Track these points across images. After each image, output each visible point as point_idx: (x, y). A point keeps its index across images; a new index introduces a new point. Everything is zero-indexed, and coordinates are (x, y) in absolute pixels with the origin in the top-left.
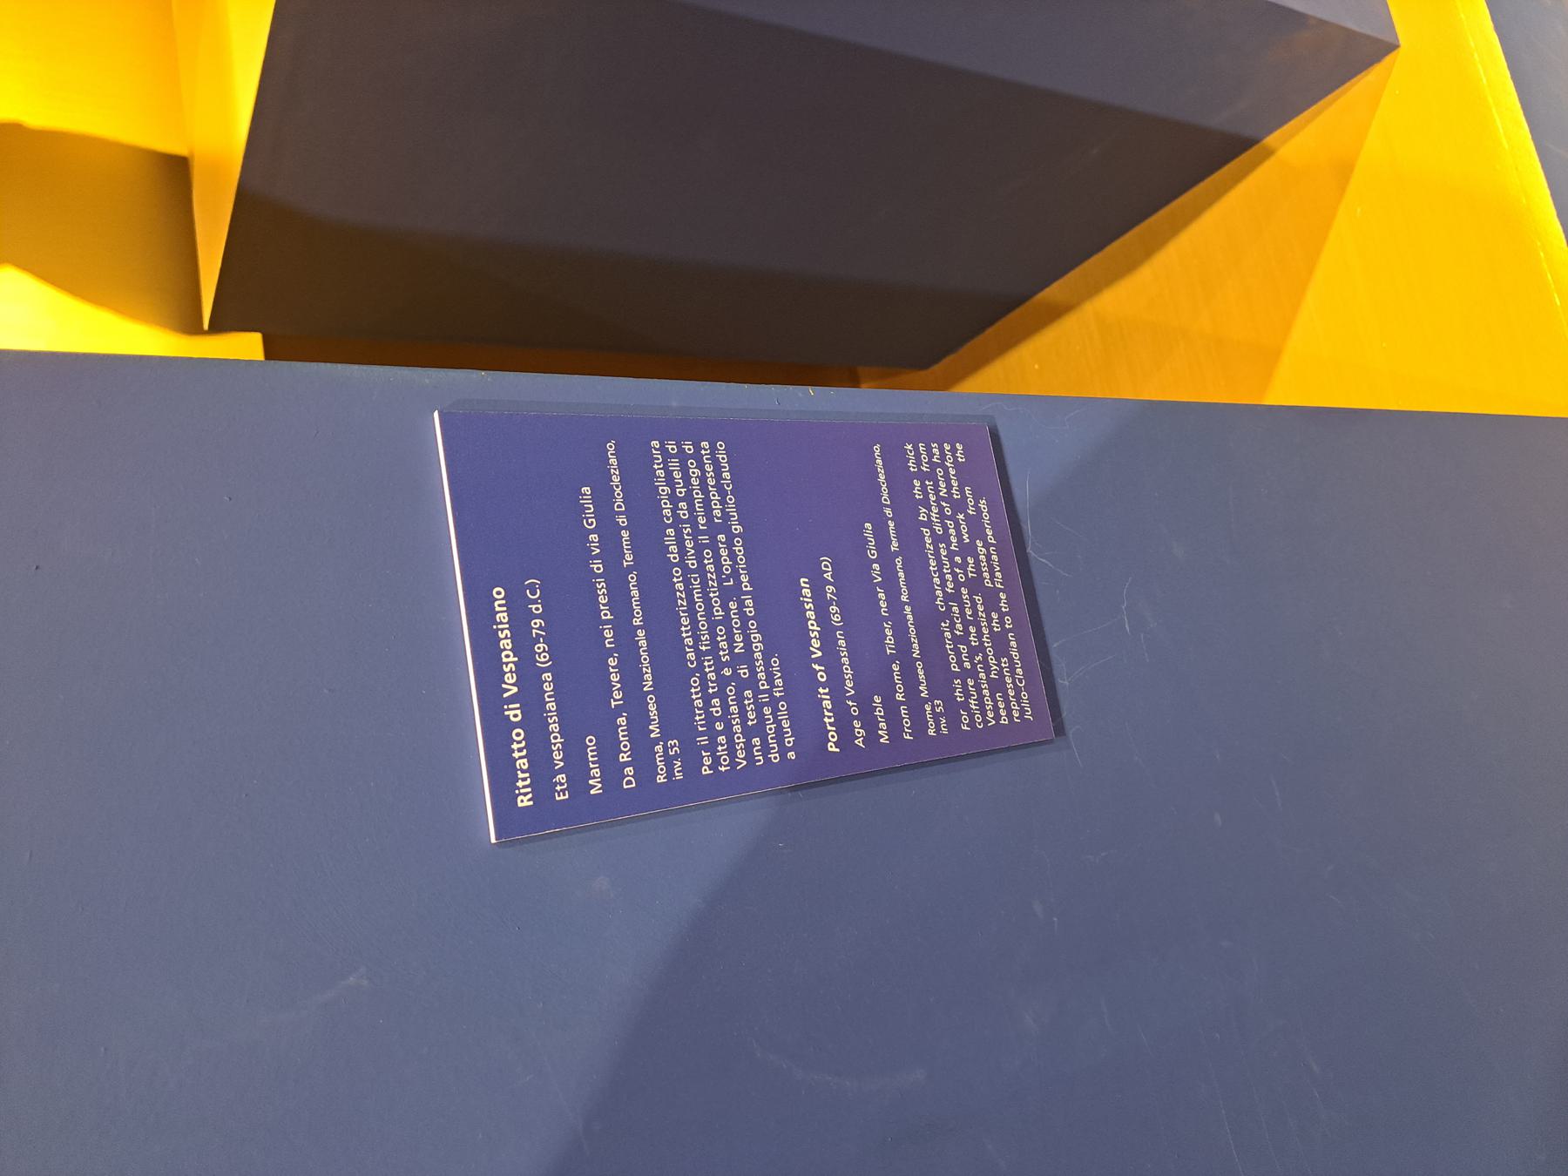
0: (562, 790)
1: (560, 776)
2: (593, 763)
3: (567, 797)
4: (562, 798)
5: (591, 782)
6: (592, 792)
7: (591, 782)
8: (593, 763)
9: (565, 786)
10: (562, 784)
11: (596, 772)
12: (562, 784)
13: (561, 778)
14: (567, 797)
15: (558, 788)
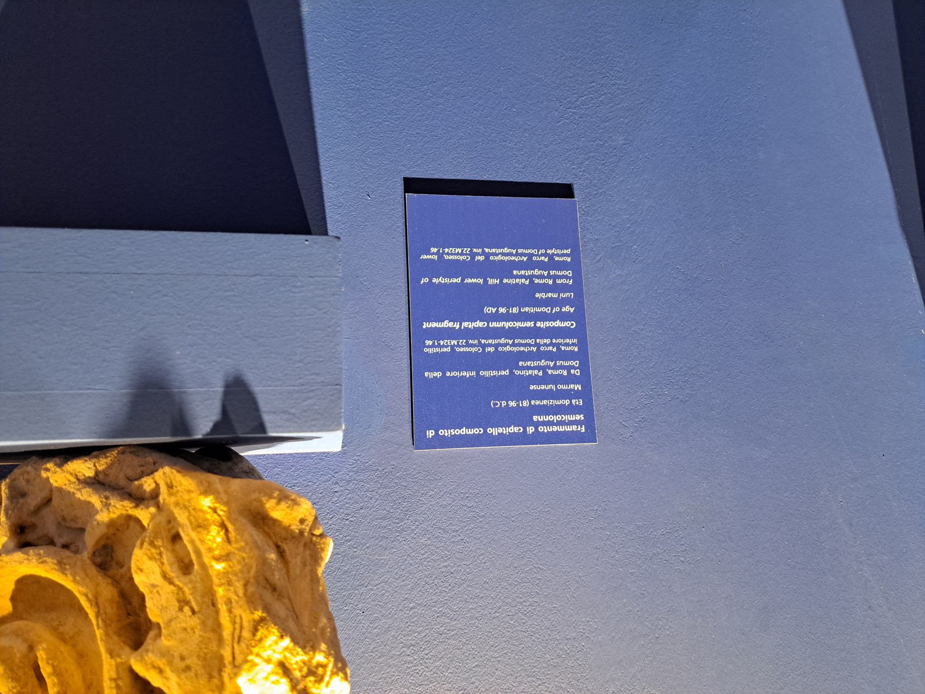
0: (579, 401)
1: (573, 402)
2: (568, 387)
3: (581, 400)
4: (581, 402)
5: (576, 389)
6: (580, 389)
7: (576, 389)
8: (568, 387)
9: (577, 400)
10: (576, 402)
11: (572, 386)
12: (576, 402)
13: (573, 401)
14: (581, 400)
15: (577, 403)
